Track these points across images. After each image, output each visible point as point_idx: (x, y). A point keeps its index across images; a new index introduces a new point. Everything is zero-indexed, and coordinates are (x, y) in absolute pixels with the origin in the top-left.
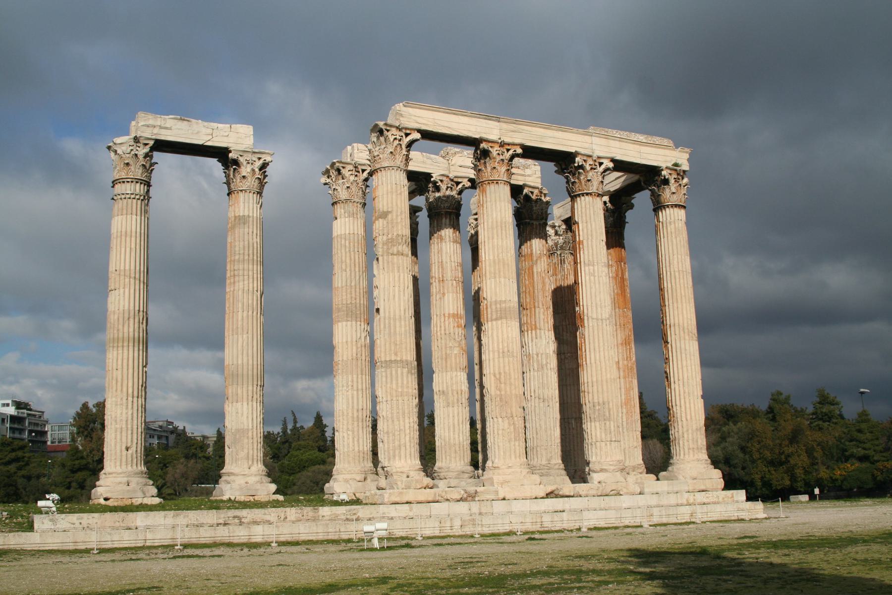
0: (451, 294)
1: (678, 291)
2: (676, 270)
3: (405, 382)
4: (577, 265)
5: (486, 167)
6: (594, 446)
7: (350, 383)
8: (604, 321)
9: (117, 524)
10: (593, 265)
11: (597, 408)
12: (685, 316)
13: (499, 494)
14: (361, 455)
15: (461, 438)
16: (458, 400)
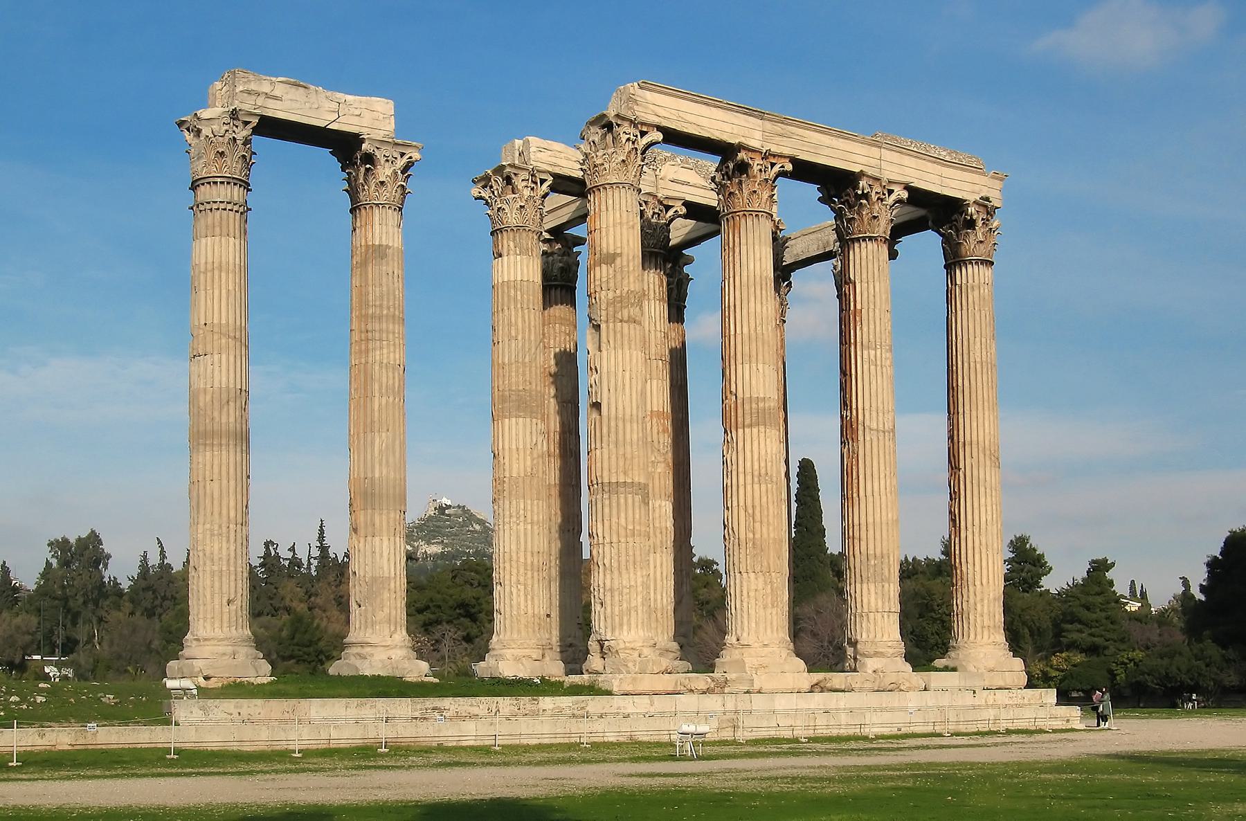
0: (655, 382)
1: (980, 392)
2: (978, 360)
3: (637, 516)
4: (850, 346)
5: (741, 190)
6: (865, 618)
7: (522, 512)
8: (886, 434)
9: (286, 716)
10: (875, 349)
11: (872, 563)
12: (987, 431)
13: (755, 686)
14: (537, 620)
15: (665, 600)
16: (661, 542)
